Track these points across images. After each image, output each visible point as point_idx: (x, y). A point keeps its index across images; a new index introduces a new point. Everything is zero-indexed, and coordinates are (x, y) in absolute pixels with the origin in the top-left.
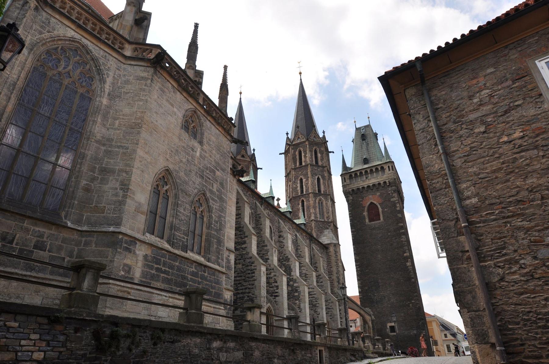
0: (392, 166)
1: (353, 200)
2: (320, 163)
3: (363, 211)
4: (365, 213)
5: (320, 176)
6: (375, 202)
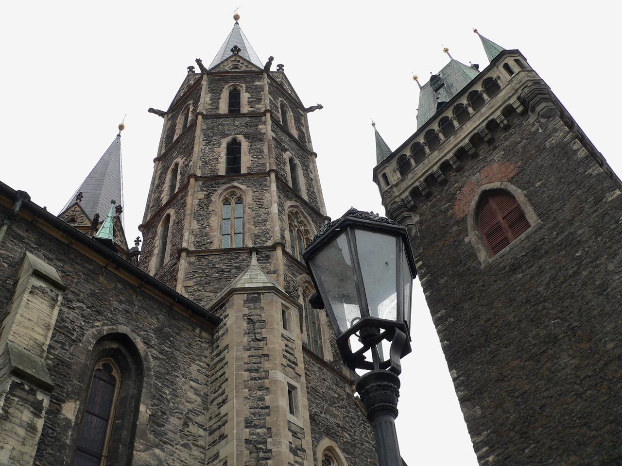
0: (517, 61)
1: (421, 222)
2: (245, 109)
3: (464, 232)
4: (472, 237)
5: (240, 138)
6: (496, 185)
